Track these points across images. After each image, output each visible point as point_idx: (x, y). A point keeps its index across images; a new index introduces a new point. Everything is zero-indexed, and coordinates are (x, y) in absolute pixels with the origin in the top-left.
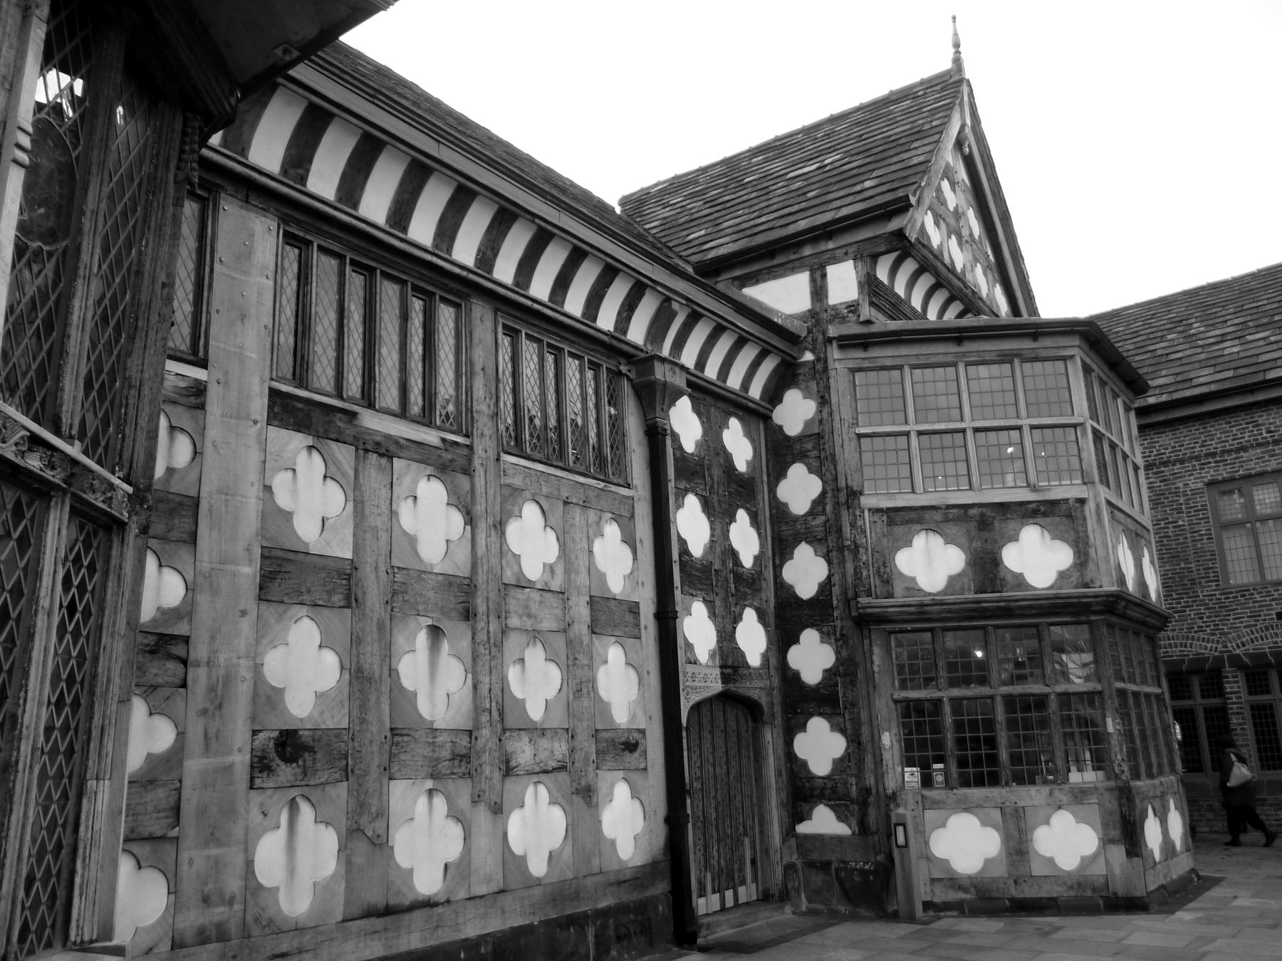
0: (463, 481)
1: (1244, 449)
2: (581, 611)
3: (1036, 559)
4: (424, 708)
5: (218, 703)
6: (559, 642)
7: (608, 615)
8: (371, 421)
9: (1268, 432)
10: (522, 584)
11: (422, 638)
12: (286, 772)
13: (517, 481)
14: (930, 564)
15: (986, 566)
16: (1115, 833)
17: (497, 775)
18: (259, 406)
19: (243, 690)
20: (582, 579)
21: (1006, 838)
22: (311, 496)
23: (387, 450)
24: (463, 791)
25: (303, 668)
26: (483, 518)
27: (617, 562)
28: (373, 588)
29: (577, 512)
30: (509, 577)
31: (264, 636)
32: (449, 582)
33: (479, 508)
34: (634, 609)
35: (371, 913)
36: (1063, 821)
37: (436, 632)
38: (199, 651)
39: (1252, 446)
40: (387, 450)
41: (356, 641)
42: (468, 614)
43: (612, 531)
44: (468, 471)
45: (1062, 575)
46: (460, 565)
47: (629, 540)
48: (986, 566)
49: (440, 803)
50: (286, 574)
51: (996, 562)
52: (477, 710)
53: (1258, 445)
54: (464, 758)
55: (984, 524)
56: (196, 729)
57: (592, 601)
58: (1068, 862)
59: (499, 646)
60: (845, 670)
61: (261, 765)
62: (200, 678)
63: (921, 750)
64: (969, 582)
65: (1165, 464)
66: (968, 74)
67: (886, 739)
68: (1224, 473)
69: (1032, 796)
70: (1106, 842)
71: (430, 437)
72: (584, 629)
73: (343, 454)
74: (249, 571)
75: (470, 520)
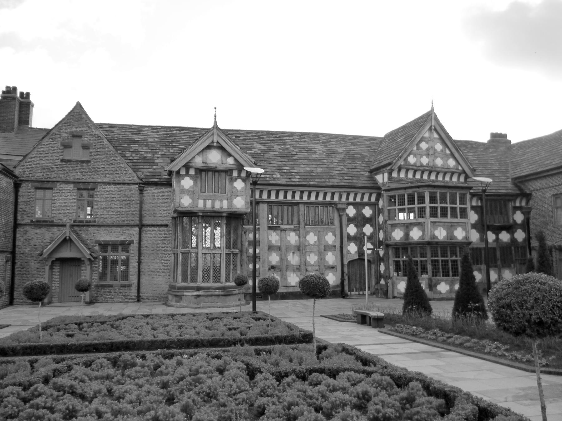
0: (298, 232)
2: (323, 247)
3: (416, 234)
4: (292, 263)
5: (264, 263)
6: (317, 253)
7: (328, 248)
8: (282, 227)
10: (309, 245)
11: (291, 254)
12: (272, 270)
13: (309, 230)
14: (398, 235)
15: (407, 235)
17: (304, 272)
18: (267, 228)
19: (266, 261)
20: (323, 243)
22: (274, 238)
23: (284, 230)
24: (299, 273)
25: (274, 258)
26: (302, 236)
27: (330, 238)
28: (283, 248)
29: (322, 233)
30: (307, 244)
31: (269, 255)
32: (296, 246)
33: (301, 235)
34: (335, 246)
35: (284, 287)
37: (293, 253)
38: (261, 257)
40: (284, 230)
41: (281, 255)
42: (299, 250)
43: (330, 234)
44: (299, 230)
46: (298, 244)
47: (334, 235)
48: (407, 235)
49: (295, 275)
50: (271, 248)
52: (301, 263)
54: (299, 269)
55: (407, 227)
56: (261, 266)
57: (325, 246)
59: (305, 254)
60: (386, 254)
61: (269, 269)
62: (261, 260)
63: (397, 270)
65: (543, 189)
66: (435, 111)
67: (391, 267)
71: (292, 227)
72: (323, 250)
73: (278, 232)
74: (266, 248)
75: (299, 237)
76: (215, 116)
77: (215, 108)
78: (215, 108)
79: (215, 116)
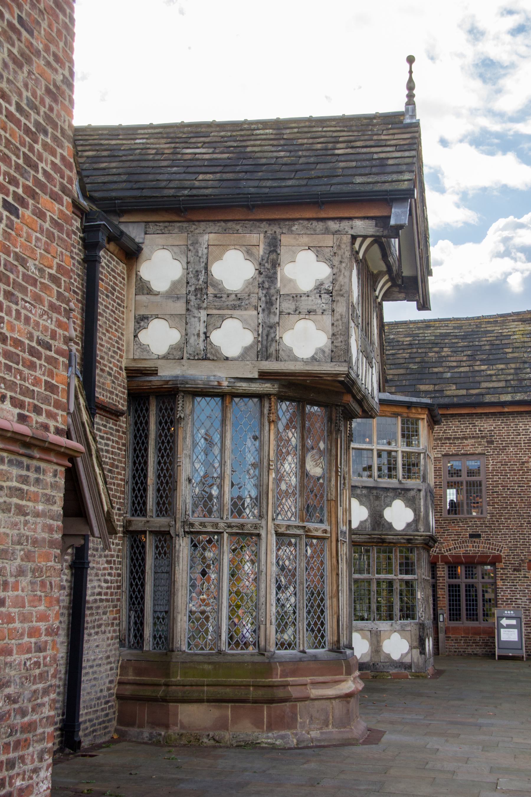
1: (466, 438)
9: (479, 431)
15: (377, 518)
16: (416, 644)
21: (371, 644)
36: (396, 637)
39: (470, 437)
45: (409, 525)
48: (377, 518)
51: (381, 516)
53: (474, 437)
58: (396, 656)
64: (368, 525)
68: (453, 450)
69: (384, 626)
70: (412, 648)
76: (411, 86)
77: (411, 60)
78: (411, 60)
79: (411, 86)
